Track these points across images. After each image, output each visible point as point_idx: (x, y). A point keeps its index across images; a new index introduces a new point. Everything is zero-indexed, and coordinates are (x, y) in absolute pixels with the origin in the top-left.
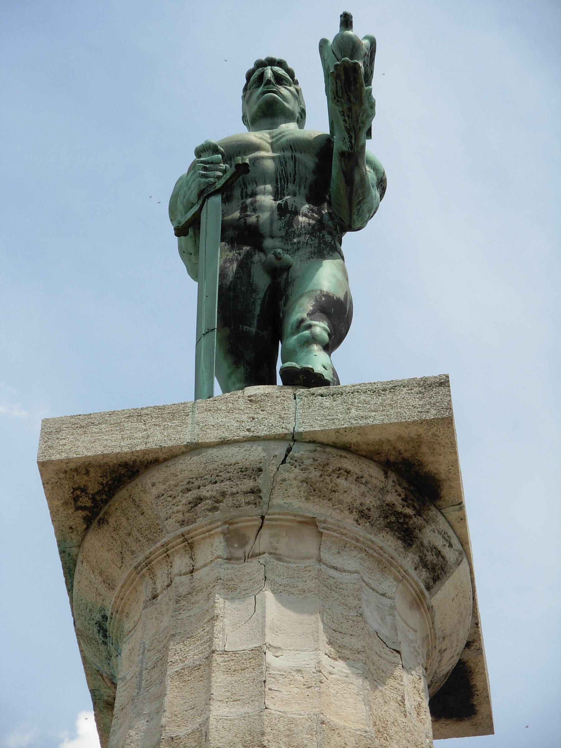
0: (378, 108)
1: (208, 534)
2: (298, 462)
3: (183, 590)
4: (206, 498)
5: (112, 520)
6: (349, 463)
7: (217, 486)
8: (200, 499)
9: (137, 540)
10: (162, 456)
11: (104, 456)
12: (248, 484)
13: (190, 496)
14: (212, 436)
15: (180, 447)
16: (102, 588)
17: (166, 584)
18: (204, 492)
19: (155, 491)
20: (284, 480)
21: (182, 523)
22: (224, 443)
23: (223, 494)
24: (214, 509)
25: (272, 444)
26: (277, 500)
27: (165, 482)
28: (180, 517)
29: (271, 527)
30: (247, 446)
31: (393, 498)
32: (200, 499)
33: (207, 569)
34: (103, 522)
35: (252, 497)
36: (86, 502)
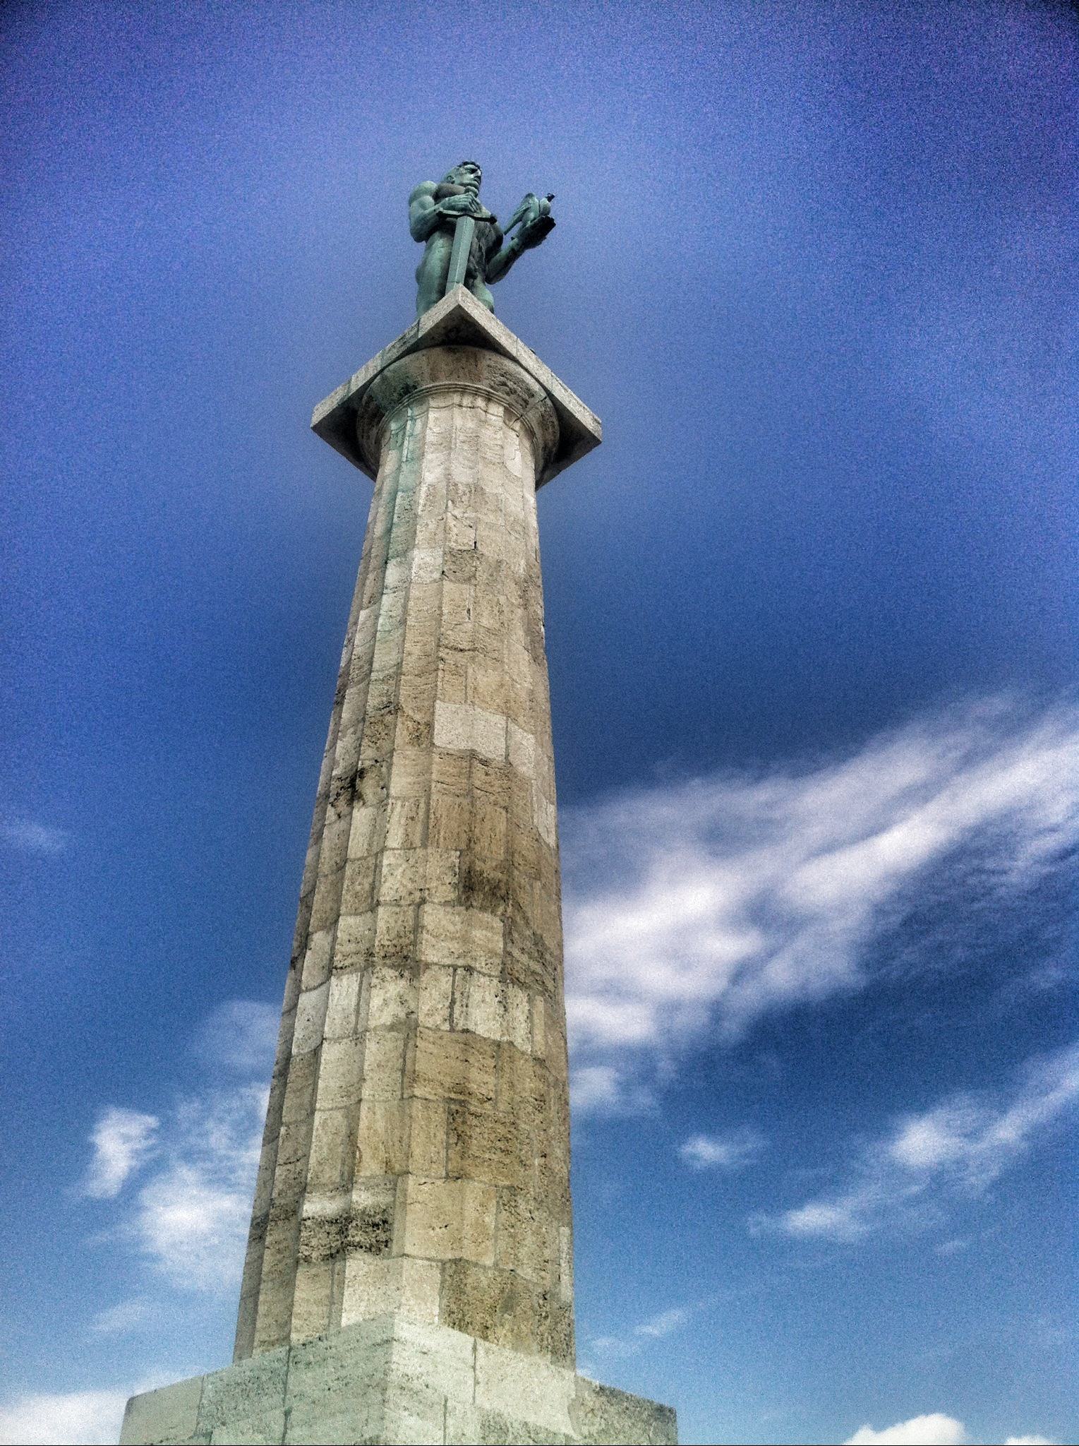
0: (538, 248)
1: (499, 403)
2: (545, 405)
3: (483, 419)
4: (508, 386)
5: (458, 355)
6: (556, 423)
7: (515, 386)
8: (504, 384)
9: (465, 374)
10: (502, 351)
11: (484, 328)
12: (526, 397)
13: (502, 379)
14: (523, 363)
15: (511, 355)
16: (426, 375)
17: (470, 405)
18: (510, 384)
19: (488, 362)
20: (537, 408)
21: (492, 387)
22: (527, 370)
23: (515, 392)
24: (508, 394)
25: (543, 390)
26: (530, 414)
27: (496, 362)
28: (492, 383)
29: (521, 422)
30: (534, 380)
31: (554, 449)
32: (504, 384)
33: (494, 418)
34: (451, 351)
35: (524, 404)
36: (453, 335)
